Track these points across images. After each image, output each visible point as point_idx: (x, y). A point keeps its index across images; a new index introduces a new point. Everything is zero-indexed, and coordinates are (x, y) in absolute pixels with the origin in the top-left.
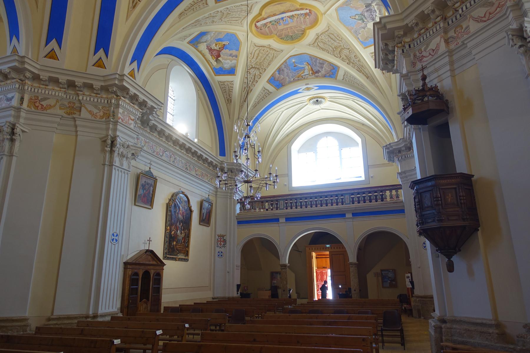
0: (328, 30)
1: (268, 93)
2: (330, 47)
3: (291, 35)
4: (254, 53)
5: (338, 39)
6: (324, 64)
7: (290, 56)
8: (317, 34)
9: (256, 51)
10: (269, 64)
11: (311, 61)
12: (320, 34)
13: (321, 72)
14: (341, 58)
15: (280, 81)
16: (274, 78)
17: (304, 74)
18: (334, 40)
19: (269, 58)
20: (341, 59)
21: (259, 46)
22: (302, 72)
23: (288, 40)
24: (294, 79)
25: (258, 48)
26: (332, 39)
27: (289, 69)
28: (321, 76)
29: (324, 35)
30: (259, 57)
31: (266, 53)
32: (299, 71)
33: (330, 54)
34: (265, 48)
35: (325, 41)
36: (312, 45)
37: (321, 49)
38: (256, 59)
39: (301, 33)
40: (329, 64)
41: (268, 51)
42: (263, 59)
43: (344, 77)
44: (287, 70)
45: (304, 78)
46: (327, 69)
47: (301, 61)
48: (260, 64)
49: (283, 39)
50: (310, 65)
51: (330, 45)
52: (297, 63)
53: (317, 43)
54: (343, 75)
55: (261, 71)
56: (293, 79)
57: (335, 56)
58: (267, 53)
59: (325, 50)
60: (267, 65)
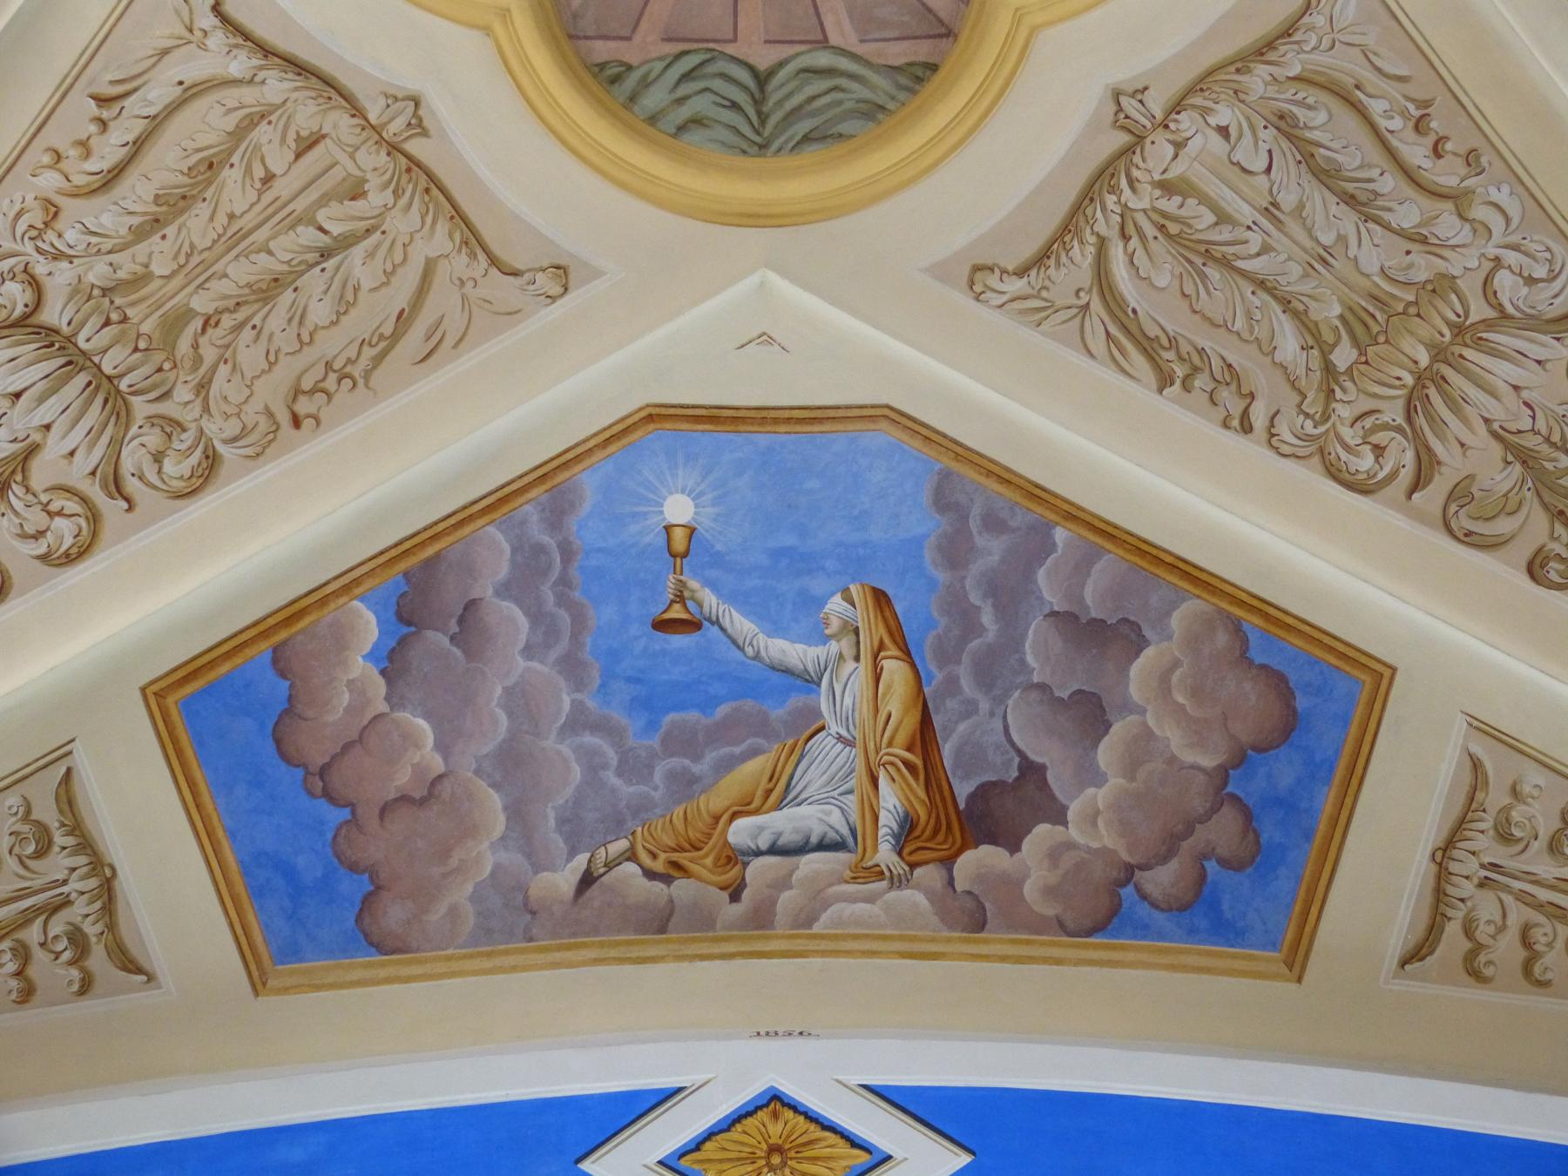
0: (1287, 31)
1: (77, 939)
2: (1278, 309)
3: (763, 58)
4: (157, 123)
5: (1409, 174)
6: (1140, 644)
7: (655, 416)
8: (1117, 95)
9: (190, 92)
10: (303, 406)
11: (942, 576)
12: (1157, 104)
13: (1059, 816)
14: (1432, 497)
15: (354, 821)
16: (290, 710)
17: (783, 823)
18: (1350, 200)
19: (344, 306)
20: (1419, 517)
21: (266, 51)
22: (755, 767)
23: (695, 136)
24: (588, 880)
25: (241, 64)
26: (1326, 175)
27: (563, 646)
28: (1049, 910)
29: (1224, 115)
30: (197, 226)
31: (324, 200)
32: (721, 732)
33: (1251, 450)
34: (340, 123)
35: (1223, 218)
36: (1016, 286)
37: (1139, 361)
38: (140, 234)
39: (899, 53)
40: (1222, 639)
41: (356, 192)
42: (241, 272)
43: (1439, 894)
44: (528, 651)
45: (762, 919)
46: (1174, 738)
47: (789, 540)
48: (170, 345)
49: (635, 76)
50: (907, 654)
51: (1292, 278)
52: (718, 560)
53: (1102, 242)
54: (1429, 835)
55: (131, 459)
56: (565, 879)
57: (1335, 473)
58: (336, 219)
59: (1187, 387)
60: (269, 413)
